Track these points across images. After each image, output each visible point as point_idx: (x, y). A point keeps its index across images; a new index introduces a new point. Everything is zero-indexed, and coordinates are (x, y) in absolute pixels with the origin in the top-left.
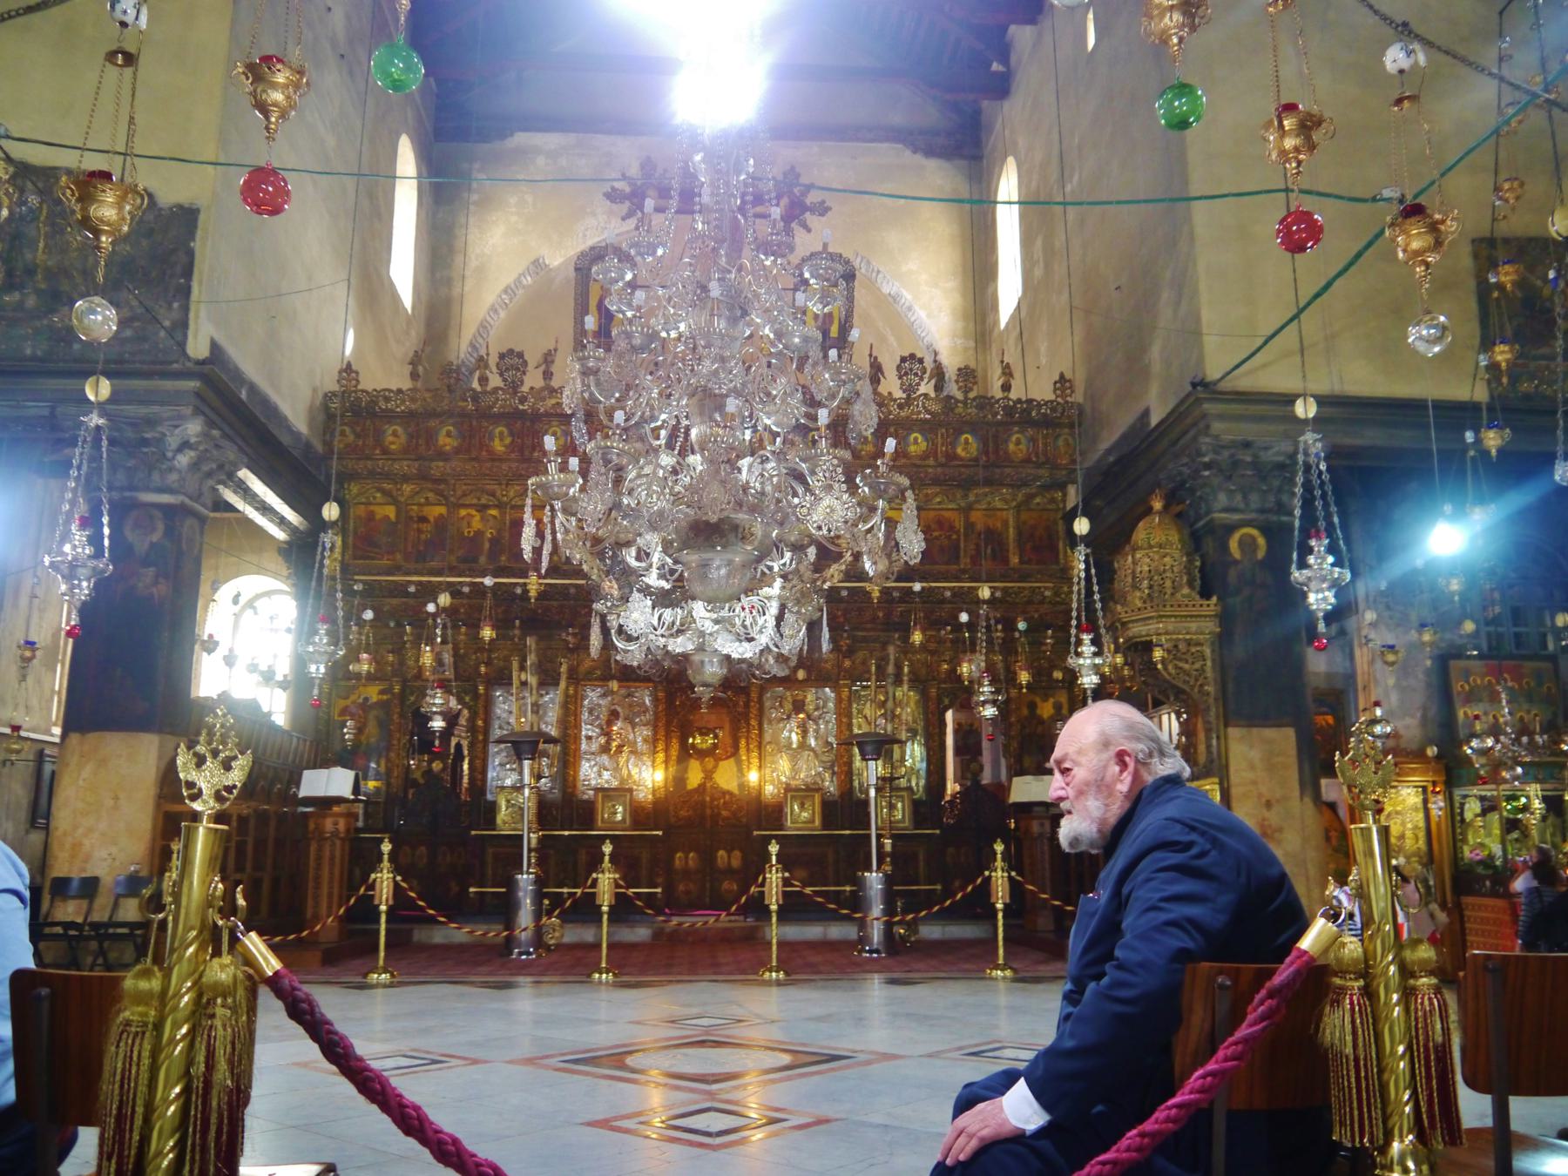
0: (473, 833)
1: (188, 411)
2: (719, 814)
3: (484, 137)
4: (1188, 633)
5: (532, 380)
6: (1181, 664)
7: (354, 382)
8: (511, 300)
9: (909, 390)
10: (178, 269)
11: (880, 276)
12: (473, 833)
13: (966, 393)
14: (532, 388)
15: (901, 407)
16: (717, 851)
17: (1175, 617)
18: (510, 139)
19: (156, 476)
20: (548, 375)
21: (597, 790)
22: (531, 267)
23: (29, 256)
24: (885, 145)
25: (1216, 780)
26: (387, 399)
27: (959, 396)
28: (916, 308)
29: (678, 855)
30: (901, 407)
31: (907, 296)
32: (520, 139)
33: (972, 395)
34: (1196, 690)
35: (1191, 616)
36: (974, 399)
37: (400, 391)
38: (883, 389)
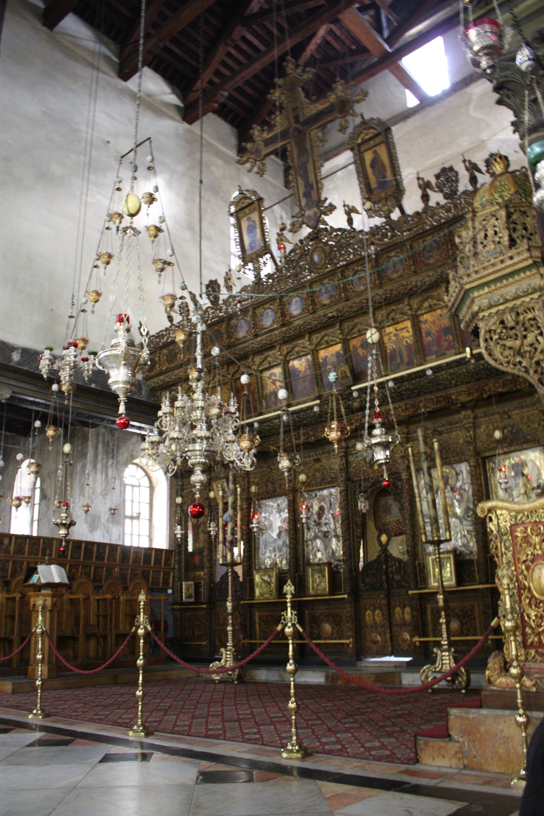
0: (242, 602)
2: (393, 578)
4: (506, 301)
5: (224, 294)
6: (509, 343)
12: (242, 602)
16: (394, 609)
17: (487, 284)
20: (229, 288)
26: (163, 336)
29: (368, 612)
30: (448, 210)
34: (531, 372)
35: (506, 277)
37: (167, 329)
38: (432, 203)
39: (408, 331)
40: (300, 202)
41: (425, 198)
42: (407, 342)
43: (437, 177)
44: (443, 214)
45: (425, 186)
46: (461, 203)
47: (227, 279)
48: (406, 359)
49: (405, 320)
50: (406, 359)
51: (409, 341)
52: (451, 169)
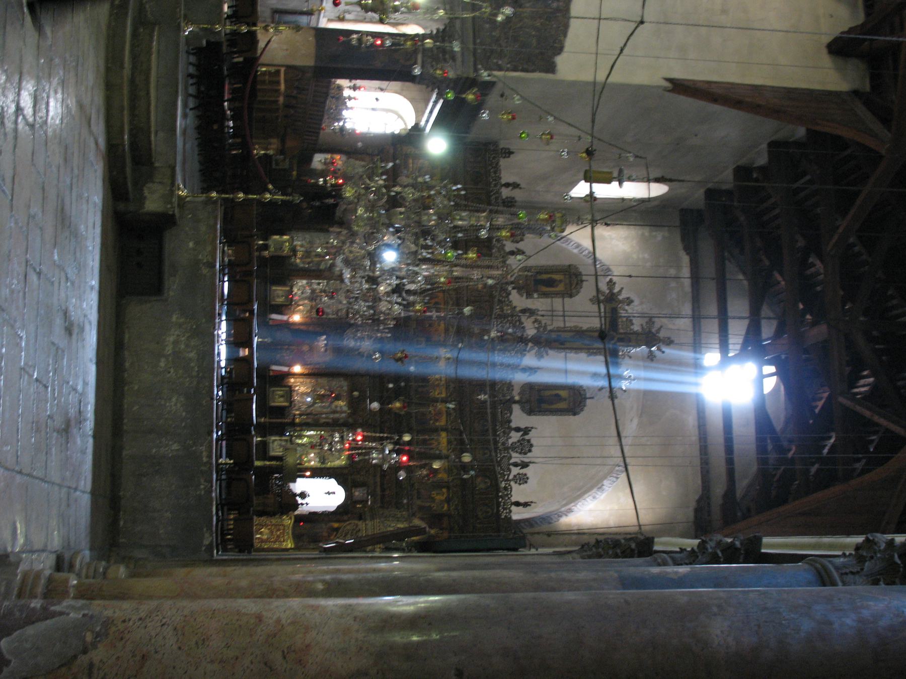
1: (459, 72)
3: (684, 238)
7: (504, 155)
8: (584, 255)
9: (513, 447)
10: (526, 66)
11: (615, 479)
13: (513, 480)
14: (504, 245)
15: (503, 444)
18: (685, 253)
19: (429, 60)
20: (512, 253)
21: (292, 287)
22: (605, 267)
23: (528, 5)
24: (700, 482)
25: (293, 546)
26: (495, 172)
27: (511, 477)
28: (596, 501)
30: (503, 444)
31: (602, 496)
32: (686, 259)
33: (512, 483)
36: (509, 485)
37: (500, 178)
39: (438, 394)
40: (555, 331)
41: (518, 429)
42: (432, 392)
43: (529, 441)
44: (502, 440)
45: (526, 431)
46: (504, 453)
47: (520, 252)
48: (420, 390)
49: (447, 394)
50: (420, 390)
51: (431, 394)
52: (530, 451)
